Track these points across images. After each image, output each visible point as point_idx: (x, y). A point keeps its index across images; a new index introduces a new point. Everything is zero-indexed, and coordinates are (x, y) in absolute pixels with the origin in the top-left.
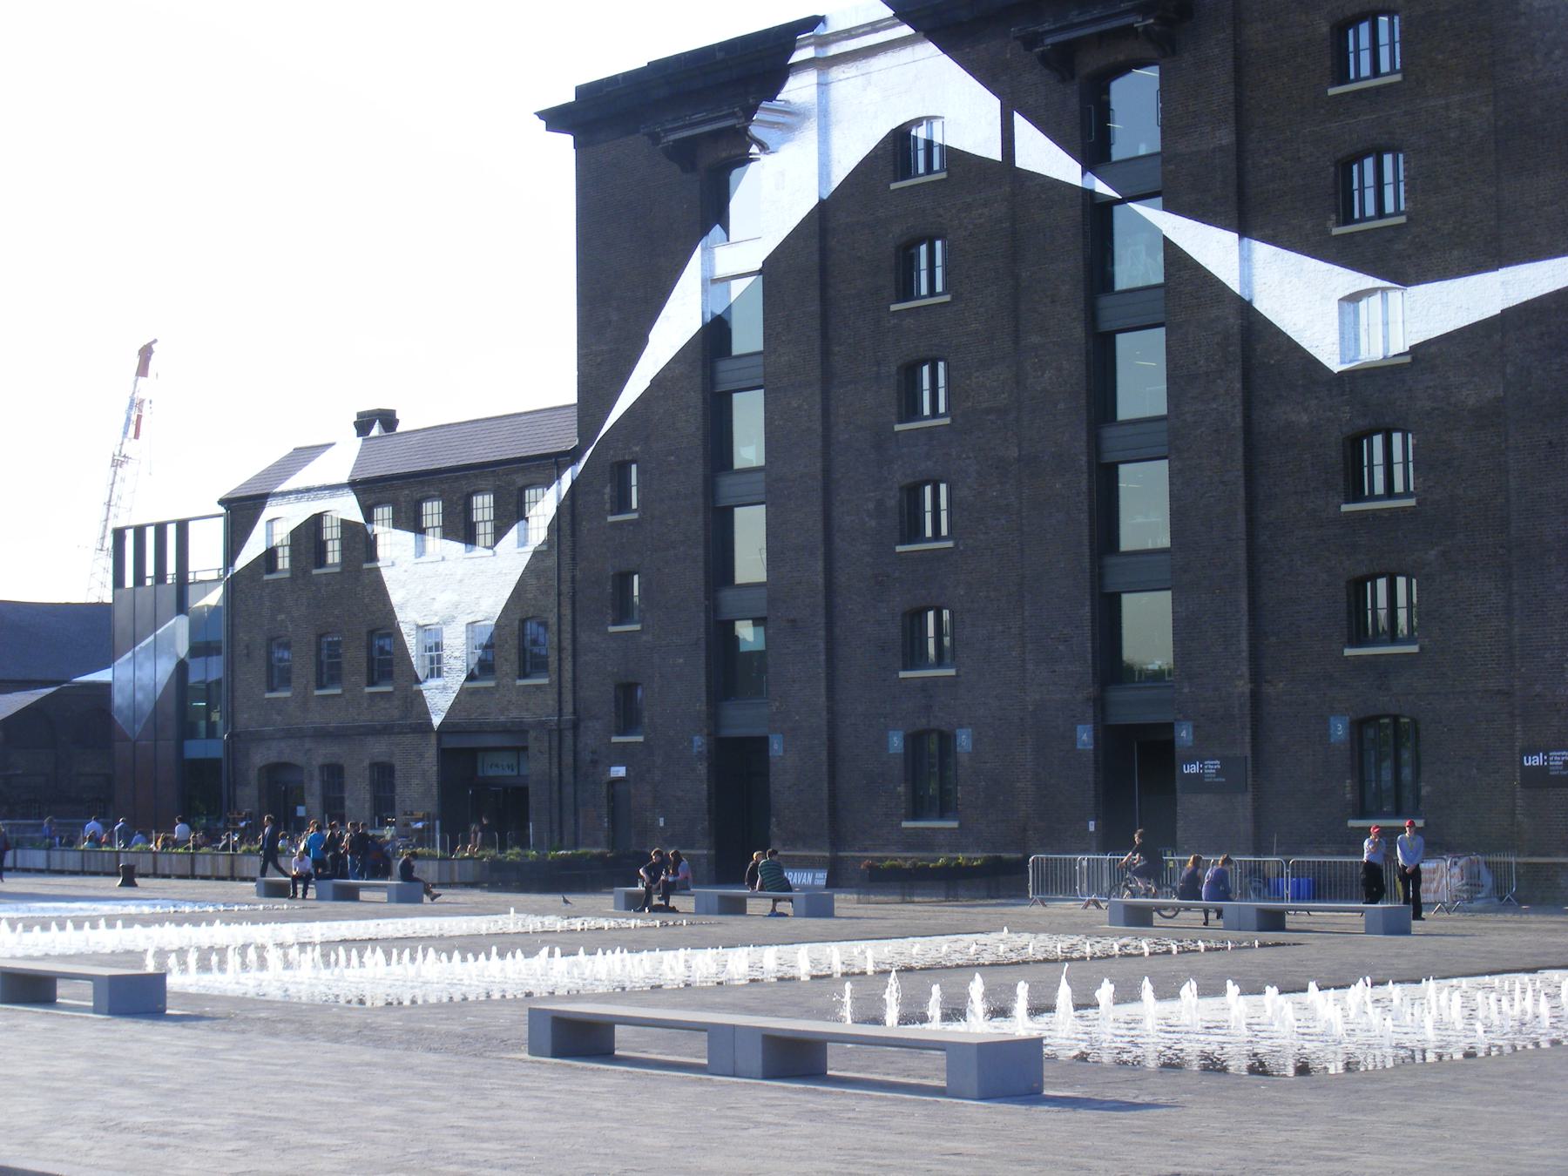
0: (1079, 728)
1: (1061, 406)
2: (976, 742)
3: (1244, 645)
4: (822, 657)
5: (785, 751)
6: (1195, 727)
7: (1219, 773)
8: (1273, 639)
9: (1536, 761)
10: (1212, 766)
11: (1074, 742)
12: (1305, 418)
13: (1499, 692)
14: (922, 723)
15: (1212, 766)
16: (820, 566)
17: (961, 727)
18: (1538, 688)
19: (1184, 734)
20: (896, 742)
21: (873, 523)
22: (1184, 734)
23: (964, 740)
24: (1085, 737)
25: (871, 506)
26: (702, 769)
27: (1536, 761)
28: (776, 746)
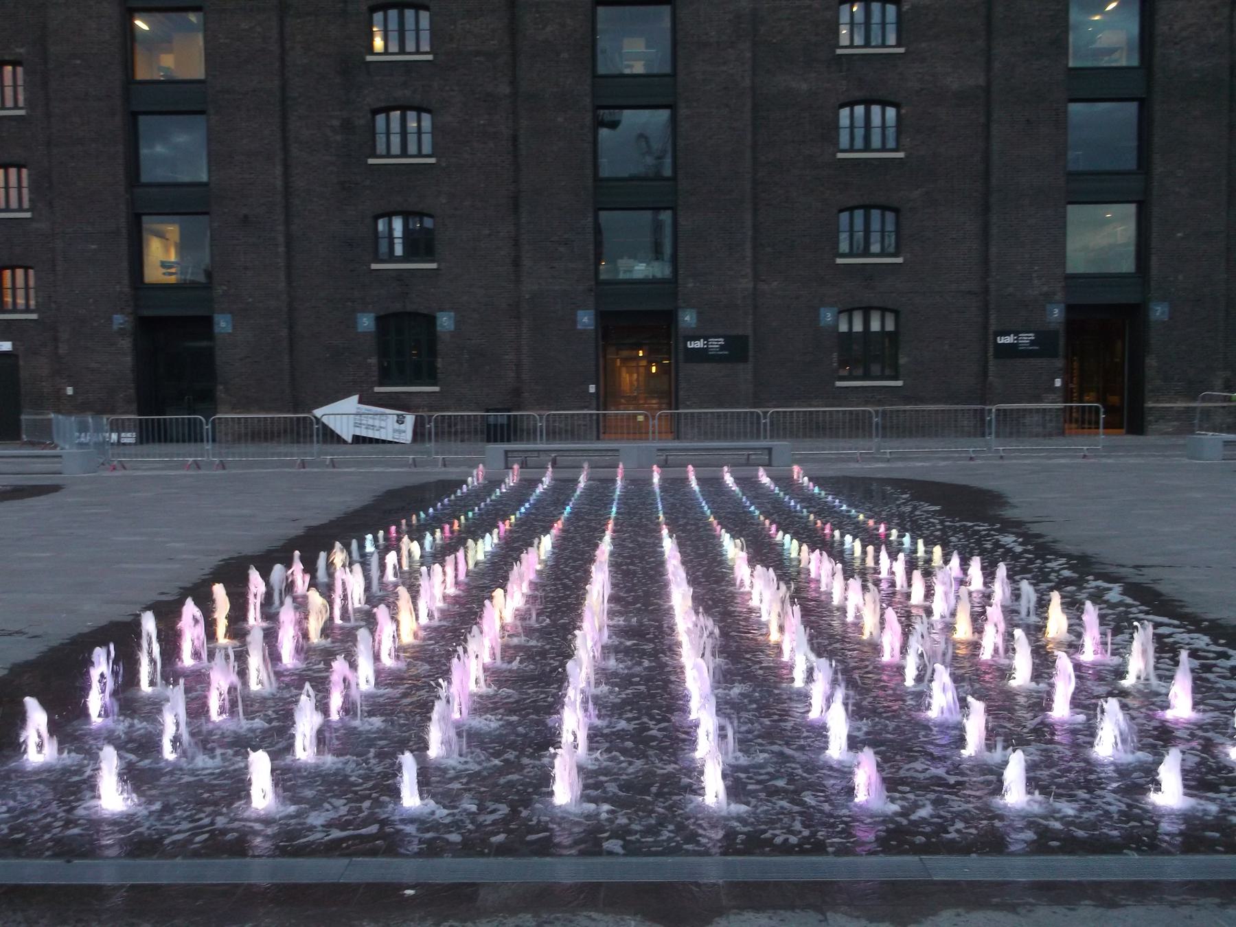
0: (580, 313)
1: (565, 55)
2: (458, 323)
3: (749, 253)
4: (281, 249)
5: (234, 327)
6: (699, 314)
7: (722, 348)
8: (769, 250)
9: (1009, 339)
10: (716, 343)
11: (575, 322)
12: (804, 86)
13: (969, 292)
14: (397, 307)
15: (716, 343)
16: (278, 170)
17: (442, 310)
18: (1011, 290)
19: (688, 318)
20: (366, 322)
21: (339, 138)
22: (688, 318)
23: (445, 322)
24: (585, 320)
25: (336, 123)
26: (126, 344)
27: (1009, 339)
28: (223, 324)
